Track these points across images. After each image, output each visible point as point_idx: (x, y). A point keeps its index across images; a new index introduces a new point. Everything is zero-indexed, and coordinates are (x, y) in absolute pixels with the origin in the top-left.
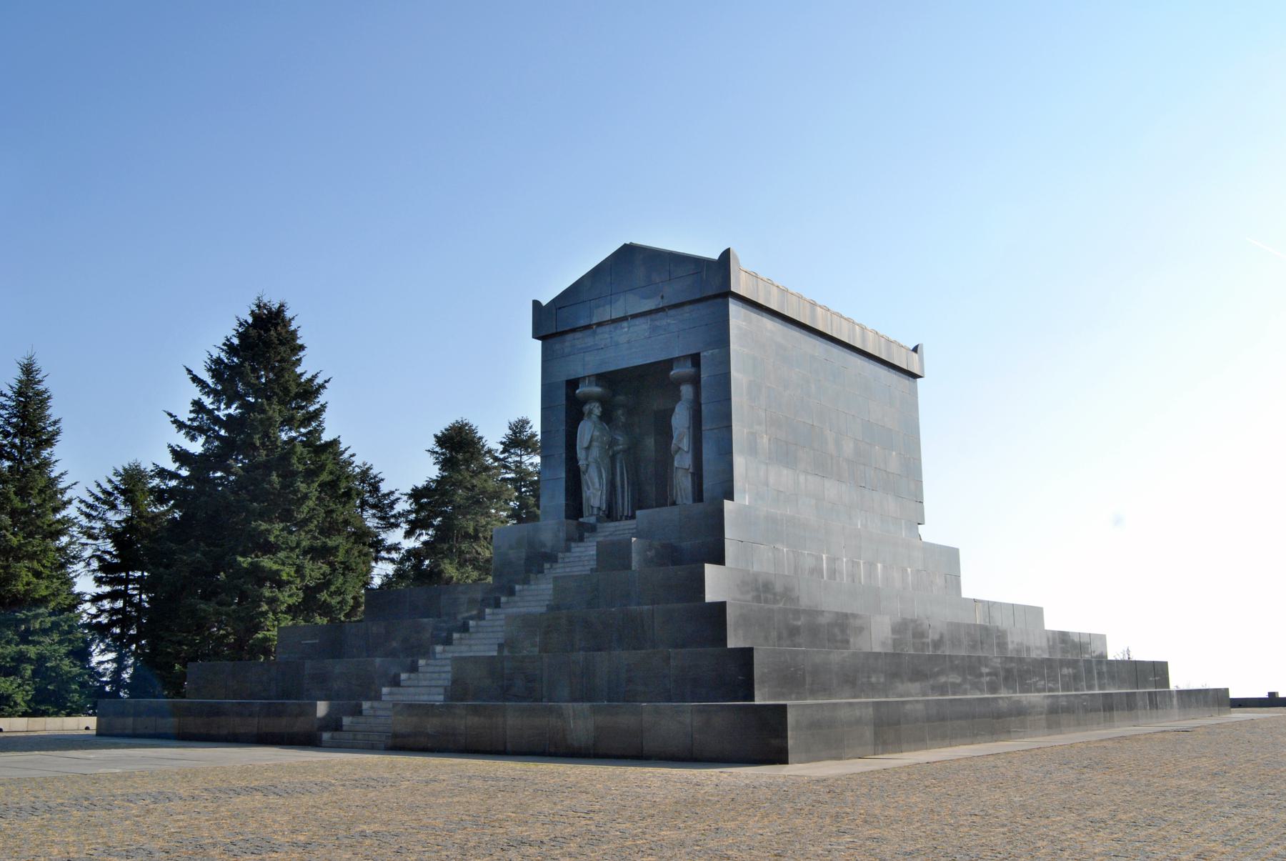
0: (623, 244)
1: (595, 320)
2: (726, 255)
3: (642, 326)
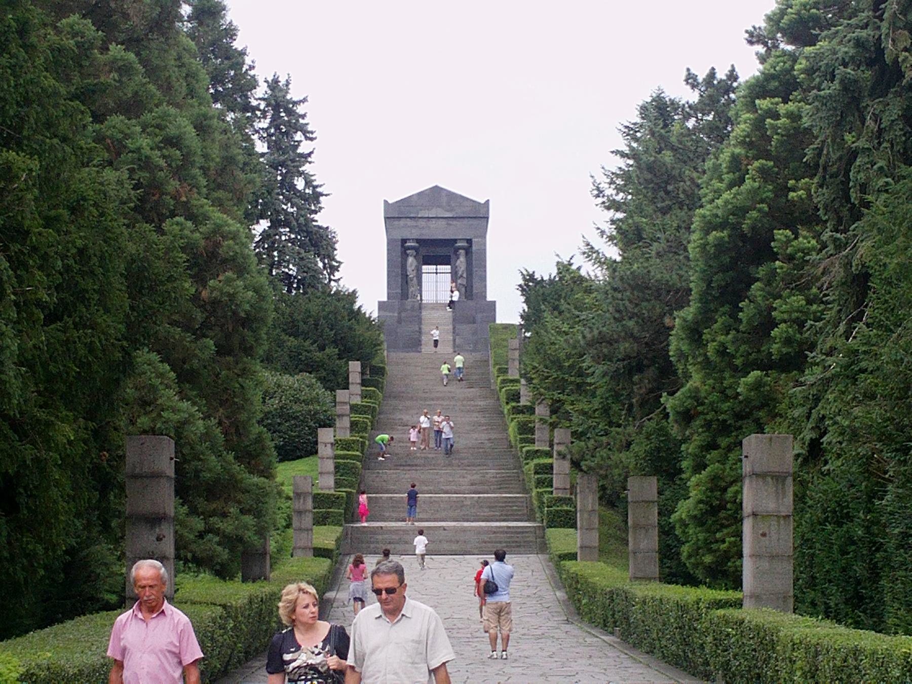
0: (434, 185)
1: (419, 216)
2: (488, 201)
3: (444, 222)
